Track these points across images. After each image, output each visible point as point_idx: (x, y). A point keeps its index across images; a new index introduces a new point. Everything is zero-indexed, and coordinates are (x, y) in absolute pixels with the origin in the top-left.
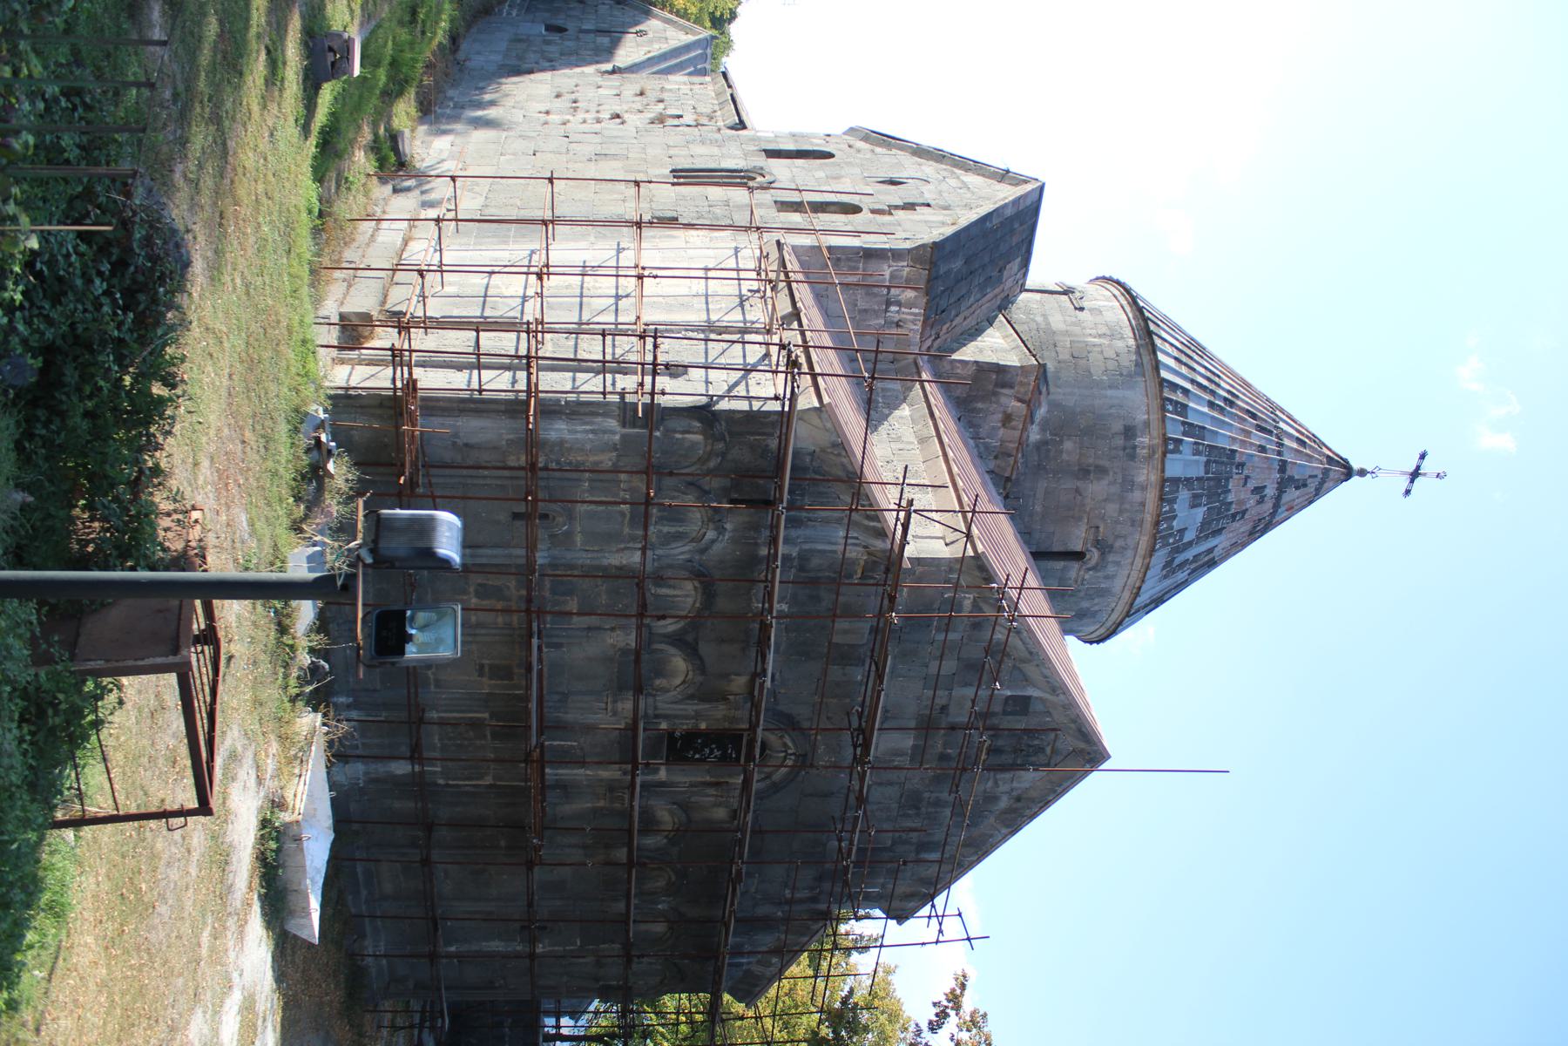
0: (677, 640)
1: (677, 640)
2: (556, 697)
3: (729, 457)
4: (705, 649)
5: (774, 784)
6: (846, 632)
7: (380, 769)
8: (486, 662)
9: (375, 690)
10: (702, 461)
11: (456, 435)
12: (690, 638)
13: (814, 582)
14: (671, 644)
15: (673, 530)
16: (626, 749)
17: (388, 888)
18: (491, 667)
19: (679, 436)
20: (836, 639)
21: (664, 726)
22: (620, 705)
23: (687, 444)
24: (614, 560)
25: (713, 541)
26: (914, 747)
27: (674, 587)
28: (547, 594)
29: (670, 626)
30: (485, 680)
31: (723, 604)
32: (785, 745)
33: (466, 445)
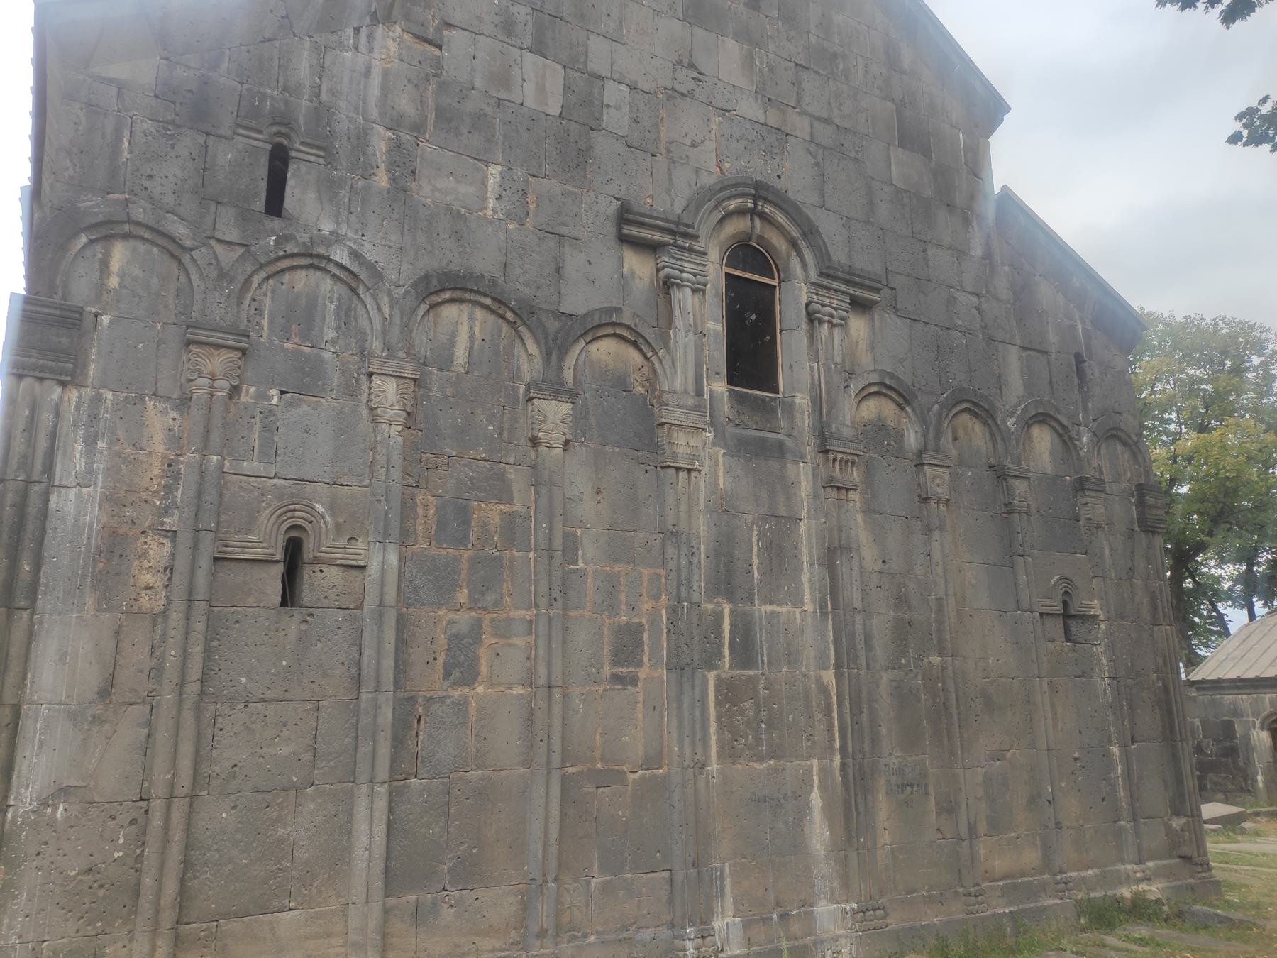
0: (555, 348)
1: (555, 348)
2: (671, 551)
3: (169, 199)
4: (577, 301)
5: (804, 235)
6: (541, 89)
7: (824, 871)
8: (607, 670)
9: (671, 882)
10: (174, 249)
11: (74, 717)
12: (553, 325)
13: (445, 117)
14: (564, 351)
15: (331, 320)
16: (760, 451)
17: (1031, 857)
18: (615, 663)
19: (114, 282)
20: (555, 110)
21: (720, 387)
22: (680, 450)
23: (137, 271)
24: (393, 432)
25: (355, 255)
26: (737, 37)
27: (454, 334)
28: (467, 554)
29: (528, 358)
30: (643, 673)
31: (485, 262)
32: (740, 212)
33: (105, 693)
